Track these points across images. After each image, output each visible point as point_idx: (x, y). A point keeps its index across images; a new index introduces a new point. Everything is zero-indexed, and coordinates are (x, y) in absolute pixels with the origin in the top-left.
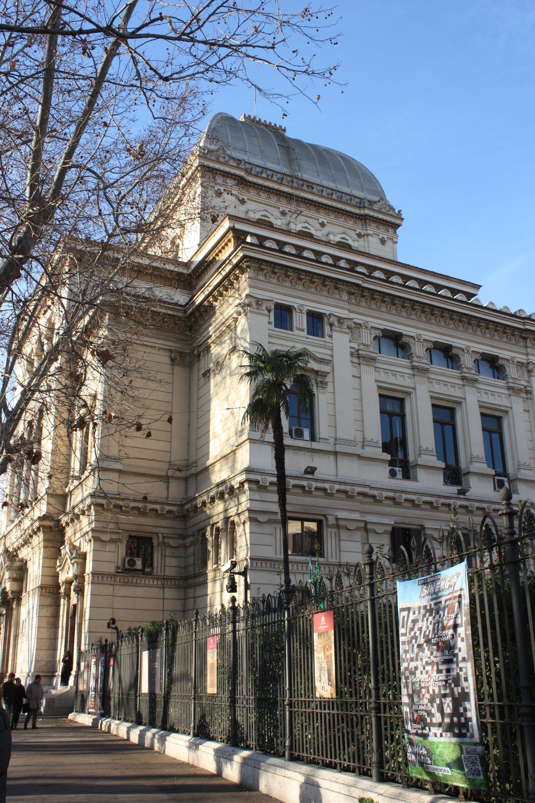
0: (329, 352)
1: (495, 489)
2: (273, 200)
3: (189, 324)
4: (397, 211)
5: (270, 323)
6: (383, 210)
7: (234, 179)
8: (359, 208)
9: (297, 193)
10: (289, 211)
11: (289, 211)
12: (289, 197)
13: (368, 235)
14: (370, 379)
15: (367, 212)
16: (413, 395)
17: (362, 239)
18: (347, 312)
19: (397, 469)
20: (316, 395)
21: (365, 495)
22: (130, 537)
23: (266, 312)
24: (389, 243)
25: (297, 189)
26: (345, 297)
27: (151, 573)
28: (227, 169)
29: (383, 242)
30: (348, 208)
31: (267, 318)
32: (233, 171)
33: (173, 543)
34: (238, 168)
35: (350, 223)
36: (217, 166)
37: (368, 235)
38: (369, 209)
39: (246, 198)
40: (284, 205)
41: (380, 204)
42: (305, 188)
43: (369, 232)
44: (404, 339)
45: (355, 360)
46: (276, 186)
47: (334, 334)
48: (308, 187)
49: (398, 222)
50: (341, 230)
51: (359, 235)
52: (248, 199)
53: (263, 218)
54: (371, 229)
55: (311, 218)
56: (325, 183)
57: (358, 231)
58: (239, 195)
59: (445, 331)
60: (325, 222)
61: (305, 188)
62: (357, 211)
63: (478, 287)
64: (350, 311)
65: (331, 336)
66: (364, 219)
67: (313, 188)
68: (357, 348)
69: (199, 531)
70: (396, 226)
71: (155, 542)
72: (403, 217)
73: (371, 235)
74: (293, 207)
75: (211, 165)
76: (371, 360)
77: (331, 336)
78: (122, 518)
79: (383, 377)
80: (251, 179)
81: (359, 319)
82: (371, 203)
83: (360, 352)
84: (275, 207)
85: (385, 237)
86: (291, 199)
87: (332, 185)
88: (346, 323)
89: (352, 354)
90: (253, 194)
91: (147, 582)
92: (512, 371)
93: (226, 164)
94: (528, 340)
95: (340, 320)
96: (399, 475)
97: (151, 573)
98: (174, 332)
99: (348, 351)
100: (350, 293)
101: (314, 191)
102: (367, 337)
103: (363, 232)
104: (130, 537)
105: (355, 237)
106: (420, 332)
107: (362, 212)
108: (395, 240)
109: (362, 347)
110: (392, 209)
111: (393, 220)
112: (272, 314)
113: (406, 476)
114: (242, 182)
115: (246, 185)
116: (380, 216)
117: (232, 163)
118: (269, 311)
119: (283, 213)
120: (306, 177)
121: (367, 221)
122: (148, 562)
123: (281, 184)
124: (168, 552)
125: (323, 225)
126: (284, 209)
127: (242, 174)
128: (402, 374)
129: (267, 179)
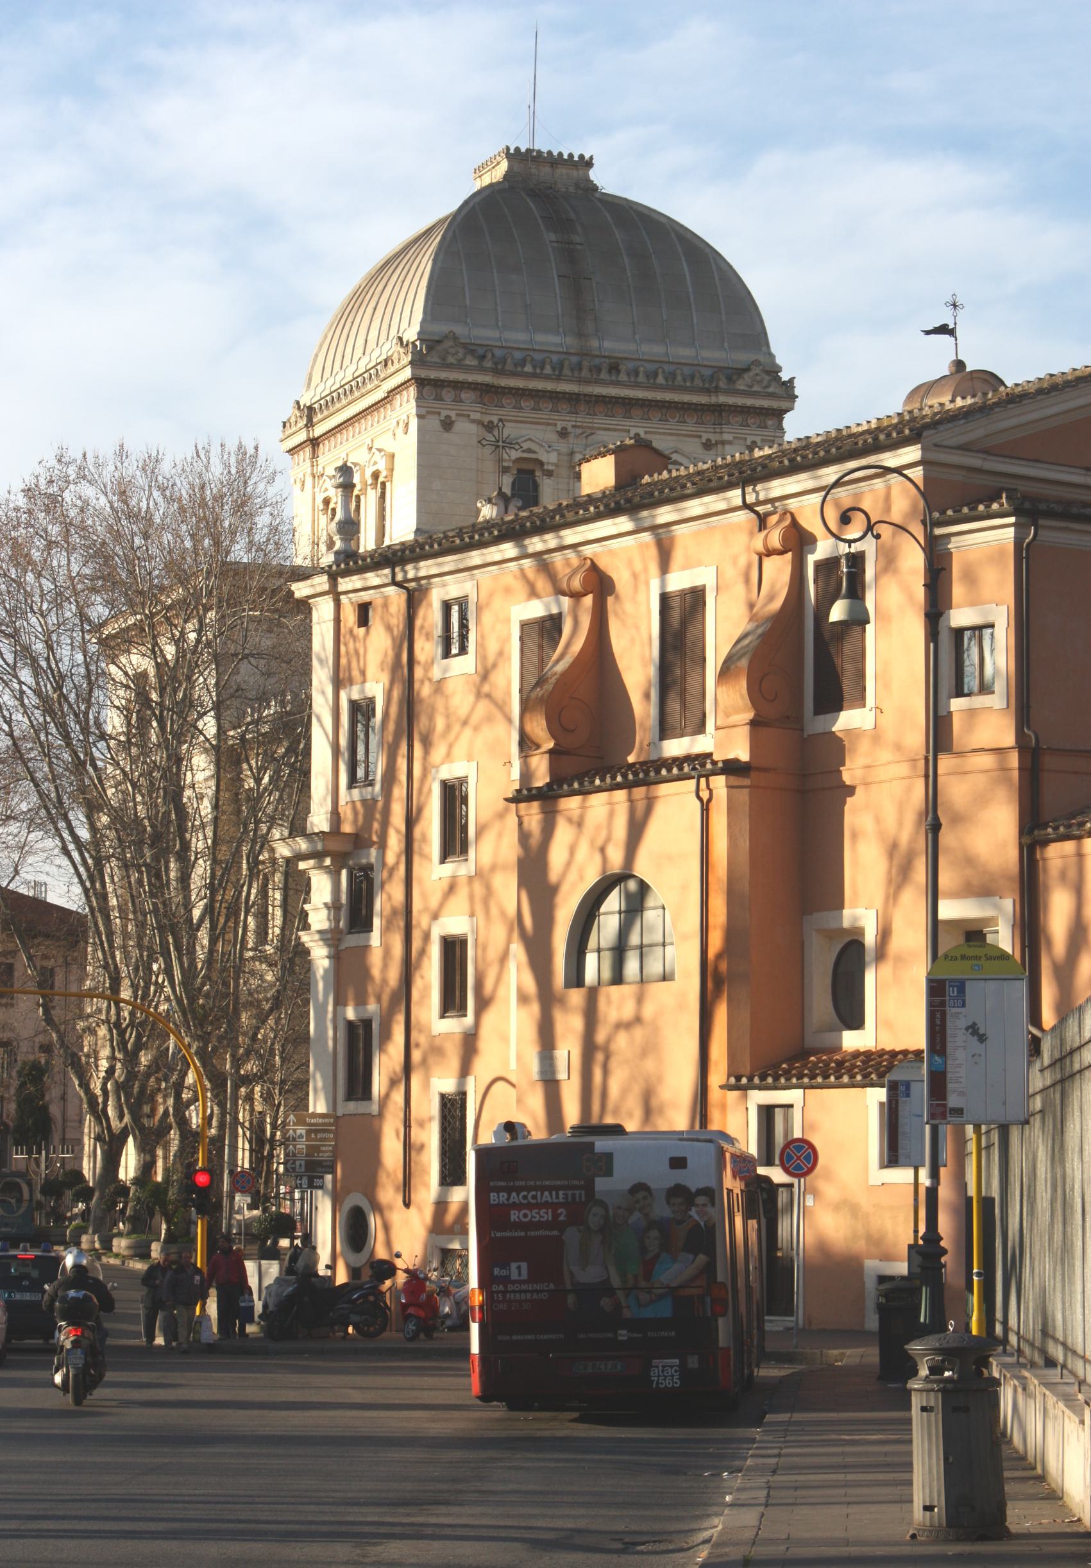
4: (785, 376)
6: (756, 388)
7: (474, 389)
8: (708, 391)
10: (574, 426)
11: (574, 426)
12: (573, 399)
13: (723, 443)
15: (723, 399)
25: (587, 382)
28: (461, 377)
30: (686, 398)
32: (471, 378)
34: (481, 369)
35: (690, 427)
36: (443, 375)
37: (723, 443)
38: (727, 392)
41: (751, 374)
42: (604, 375)
43: (726, 437)
46: (549, 386)
49: (784, 405)
53: (525, 455)
55: (615, 430)
57: (705, 437)
62: (703, 399)
66: (719, 412)
70: (779, 414)
73: (730, 443)
74: (583, 419)
75: (433, 375)
80: (504, 382)
84: (548, 424)
93: (459, 366)
103: (714, 438)
107: (713, 400)
114: (486, 392)
115: (496, 393)
116: (749, 402)
117: (470, 361)
119: (563, 434)
121: (723, 414)
127: (487, 379)
129: (533, 376)
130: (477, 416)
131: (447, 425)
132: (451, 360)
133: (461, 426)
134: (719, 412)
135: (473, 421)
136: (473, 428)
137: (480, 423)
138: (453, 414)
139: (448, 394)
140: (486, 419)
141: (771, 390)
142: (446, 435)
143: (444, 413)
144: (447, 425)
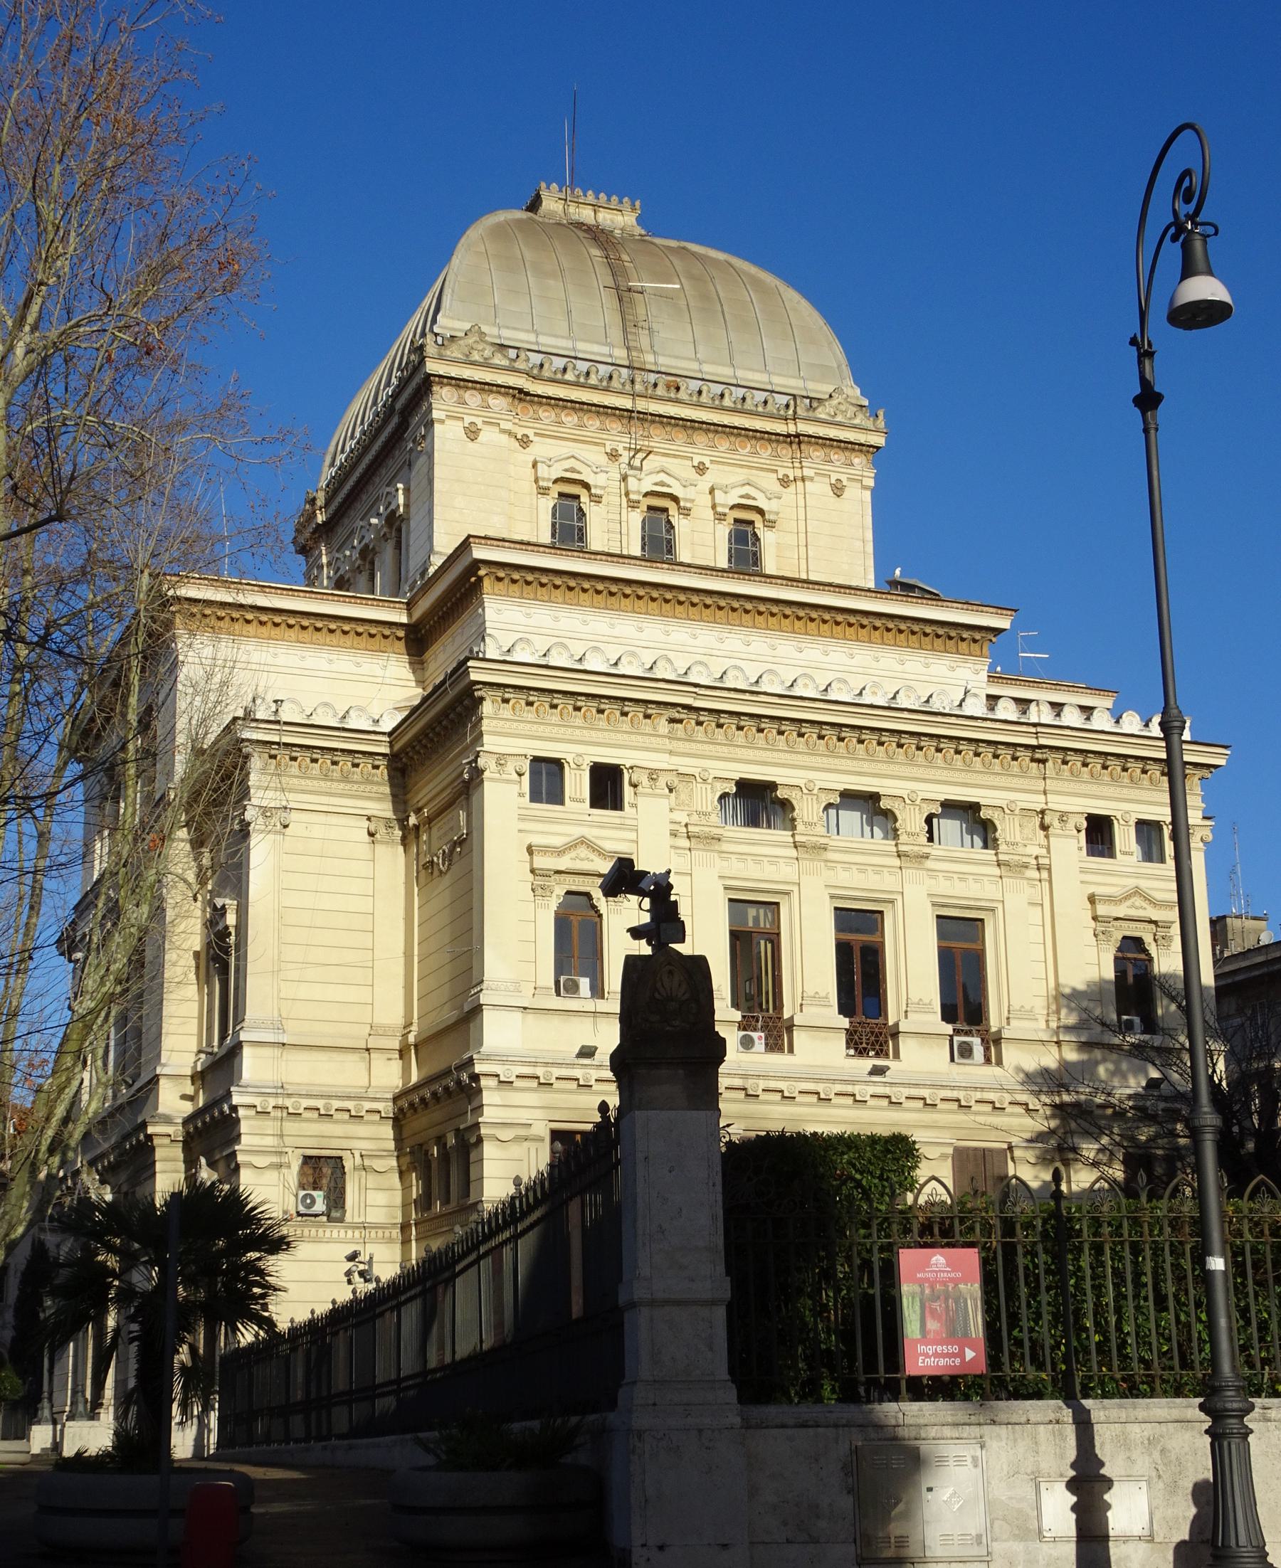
0: (633, 836)
1: (952, 1060)
3: (399, 765)
5: (521, 795)
6: (839, 418)
9: (641, 405)
15: (804, 428)
16: (795, 896)
19: (755, 1035)
20: (605, 917)
22: (307, 1159)
23: (515, 776)
26: (663, 726)
27: (341, 1220)
31: (517, 787)
32: (501, 379)
33: (378, 1164)
39: (530, 433)
41: (834, 402)
43: (807, 472)
45: (685, 843)
47: (641, 801)
48: (668, 387)
50: (740, 475)
51: (785, 482)
52: (536, 434)
53: (568, 475)
55: (675, 456)
56: (710, 370)
59: (866, 767)
60: (706, 461)
61: (660, 391)
62: (780, 428)
64: (671, 753)
65: (634, 806)
67: (678, 389)
68: (685, 820)
69: (421, 1145)
71: (348, 1165)
73: (811, 479)
77: (634, 806)
78: (291, 1127)
82: (814, 402)
83: (691, 828)
85: (844, 478)
86: (630, 418)
87: (724, 372)
89: (674, 834)
91: (335, 1234)
92: (1006, 830)
94: (1049, 764)
95: (653, 775)
96: (760, 1045)
97: (341, 1220)
98: (372, 783)
101: (682, 395)
102: (706, 798)
104: (307, 1159)
105: (777, 487)
107: (792, 429)
109: (695, 818)
112: (526, 779)
113: (774, 1045)
116: (832, 433)
117: (498, 360)
118: (520, 775)
120: (665, 363)
121: (803, 446)
122: (337, 1200)
123: (606, 390)
124: (372, 1180)
125: (701, 469)
126: (614, 445)
129: (576, 384)
130: (504, 425)
131: (472, 433)
132: (476, 357)
133: (488, 435)
134: (796, 439)
135: (503, 431)
136: (505, 437)
137: (510, 433)
138: (479, 421)
140: (520, 432)
141: (857, 421)
142: (471, 444)
143: (468, 419)
144: (472, 433)
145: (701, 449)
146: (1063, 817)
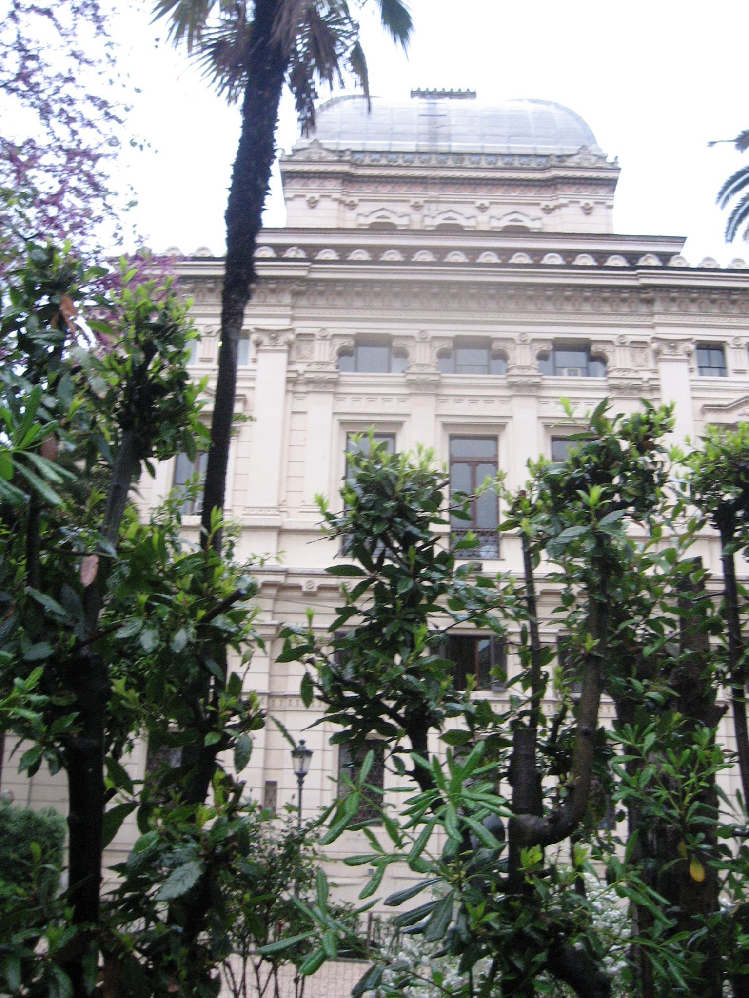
2: (401, 192)
7: (336, 178)
14: (320, 411)
15: (555, 173)
17: (552, 214)
18: (287, 321)
21: (282, 587)
24: (599, 211)
26: (287, 299)
29: (587, 210)
34: (340, 162)
35: (531, 195)
37: (559, 207)
40: (417, 195)
44: (594, 348)
47: (261, 356)
49: (611, 175)
54: (564, 195)
58: (344, 198)
63: (681, 240)
65: (255, 361)
70: (611, 184)
72: (619, 166)
73: (565, 205)
76: (328, 385)
79: (347, 406)
80: (361, 172)
81: (302, 327)
88: (282, 339)
89: (289, 381)
90: (367, 191)
99: (283, 377)
100: (296, 294)
102: (323, 353)
103: (552, 204)
106: (424, 326)
108: (609, 203)
110: (603, 158)
111: (603, 175)
114: (348, 179)
116: (578, 174)
127: (345, 168)
128: (387, 397)
130: (338, 196)
135: (335, 200)
136: (336, 204)
137: (341, 202)
139: (314, 185)
142: (312, 211)
143: (309, 196)
145: (482, 197)
146: (672, 344)
